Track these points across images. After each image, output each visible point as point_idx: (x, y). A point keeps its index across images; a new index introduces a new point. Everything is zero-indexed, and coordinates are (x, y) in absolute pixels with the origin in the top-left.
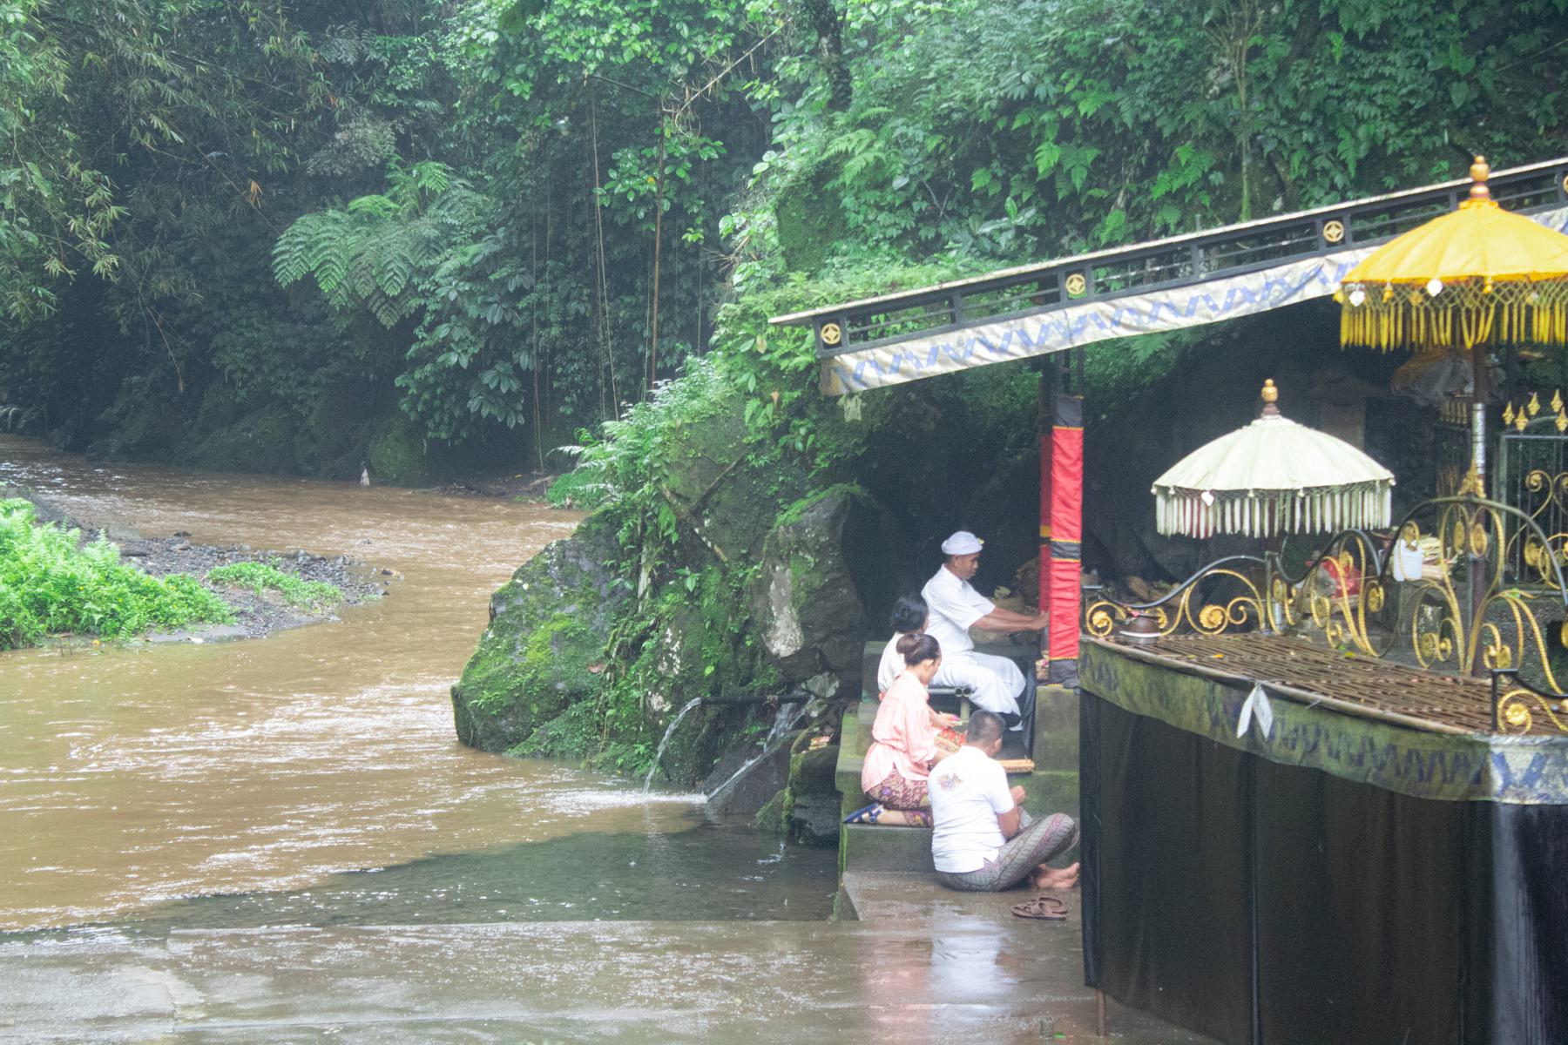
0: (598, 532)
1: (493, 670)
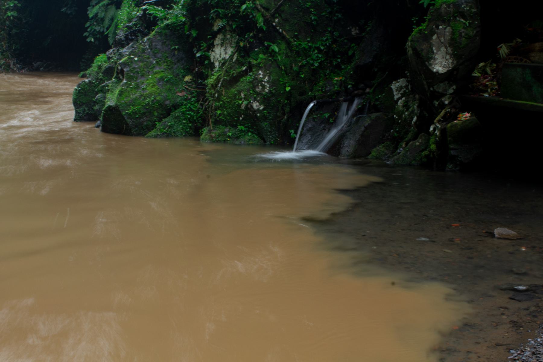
0: (166, 34)
1: (133, 97)
